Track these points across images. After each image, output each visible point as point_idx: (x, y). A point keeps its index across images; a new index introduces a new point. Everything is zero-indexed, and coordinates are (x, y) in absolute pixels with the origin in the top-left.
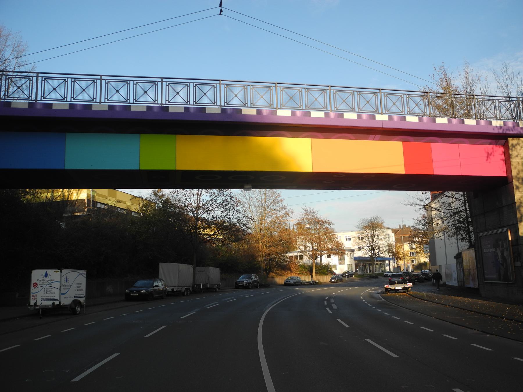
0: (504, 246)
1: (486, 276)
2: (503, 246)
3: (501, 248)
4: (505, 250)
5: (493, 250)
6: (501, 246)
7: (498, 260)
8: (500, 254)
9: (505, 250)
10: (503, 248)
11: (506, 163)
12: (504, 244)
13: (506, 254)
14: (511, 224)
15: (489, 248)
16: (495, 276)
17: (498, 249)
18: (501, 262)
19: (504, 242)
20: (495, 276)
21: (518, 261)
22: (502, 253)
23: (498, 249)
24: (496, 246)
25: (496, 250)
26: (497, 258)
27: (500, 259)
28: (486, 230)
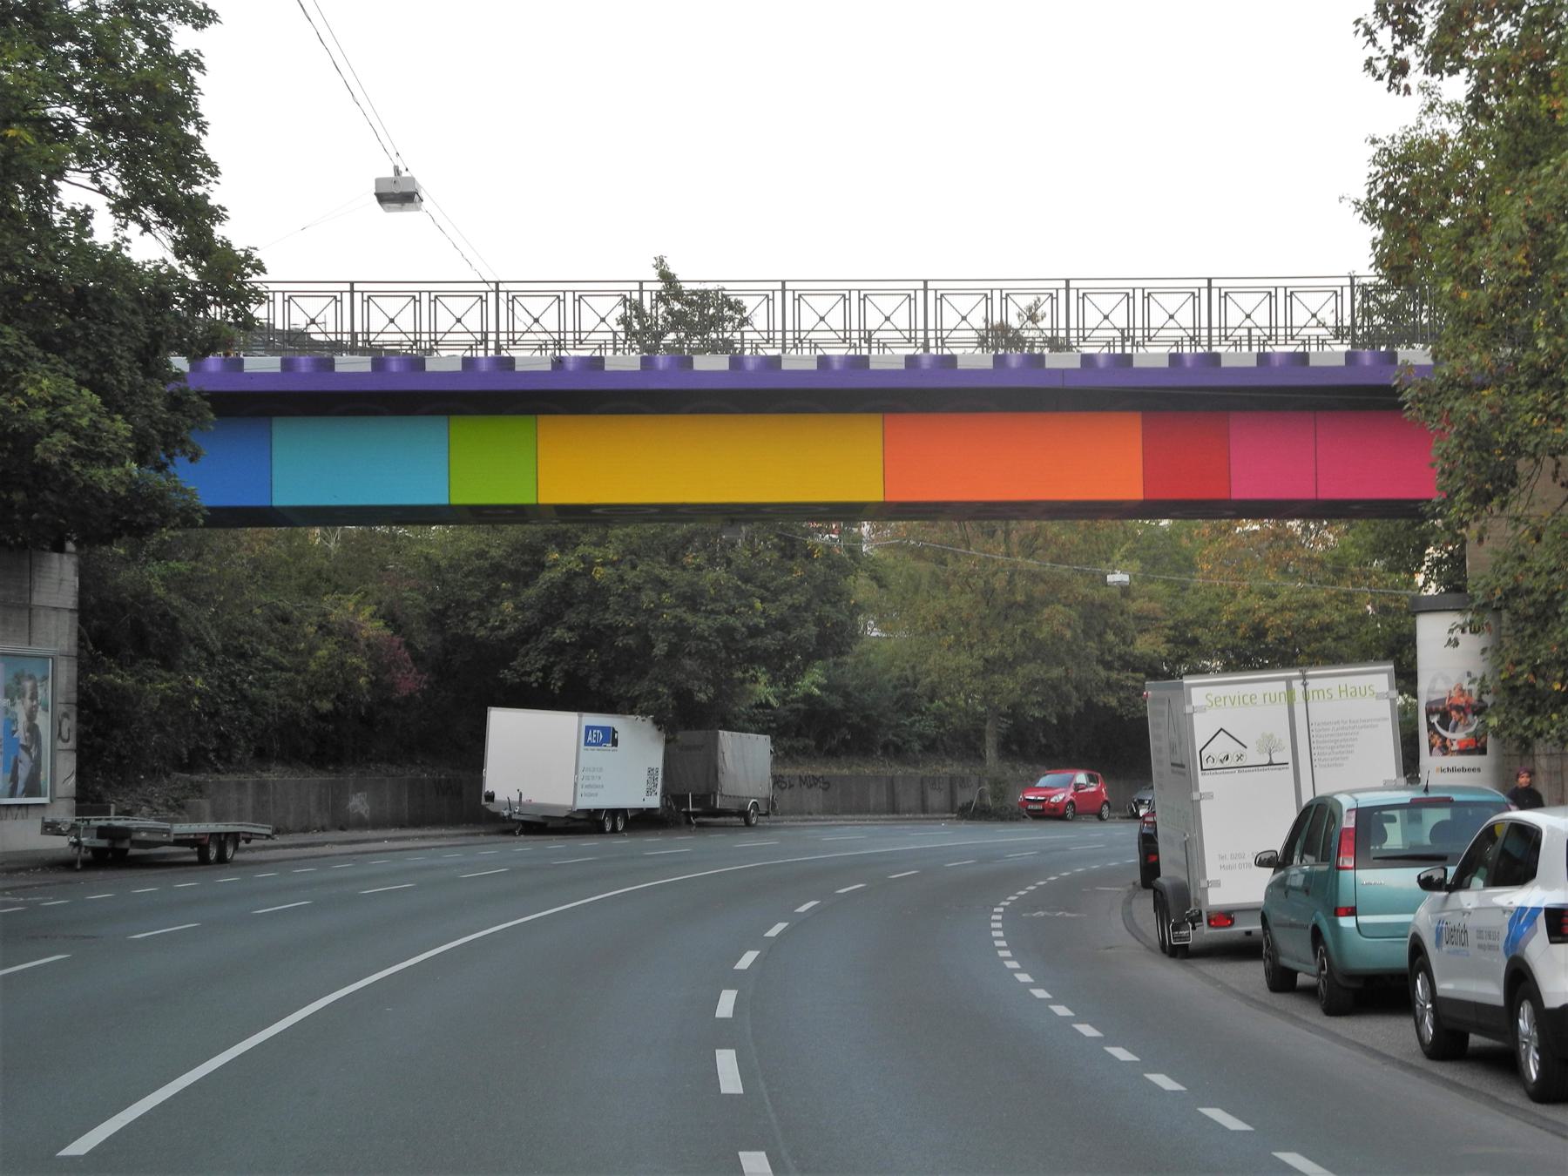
0: (39, 698)
2: (34, 697)
3: (28, 702)
6: (28, 694)
7: (15, 736)
8: (22, 719)
9: (40, 708)
10: (35, 703)
12: (40, 691)
17: (18, 701)
18: (22, 742)
22: (31, 716)
23: (18, 701)
25: (13, 704)
26: (14, 729)
27: (21, 734)
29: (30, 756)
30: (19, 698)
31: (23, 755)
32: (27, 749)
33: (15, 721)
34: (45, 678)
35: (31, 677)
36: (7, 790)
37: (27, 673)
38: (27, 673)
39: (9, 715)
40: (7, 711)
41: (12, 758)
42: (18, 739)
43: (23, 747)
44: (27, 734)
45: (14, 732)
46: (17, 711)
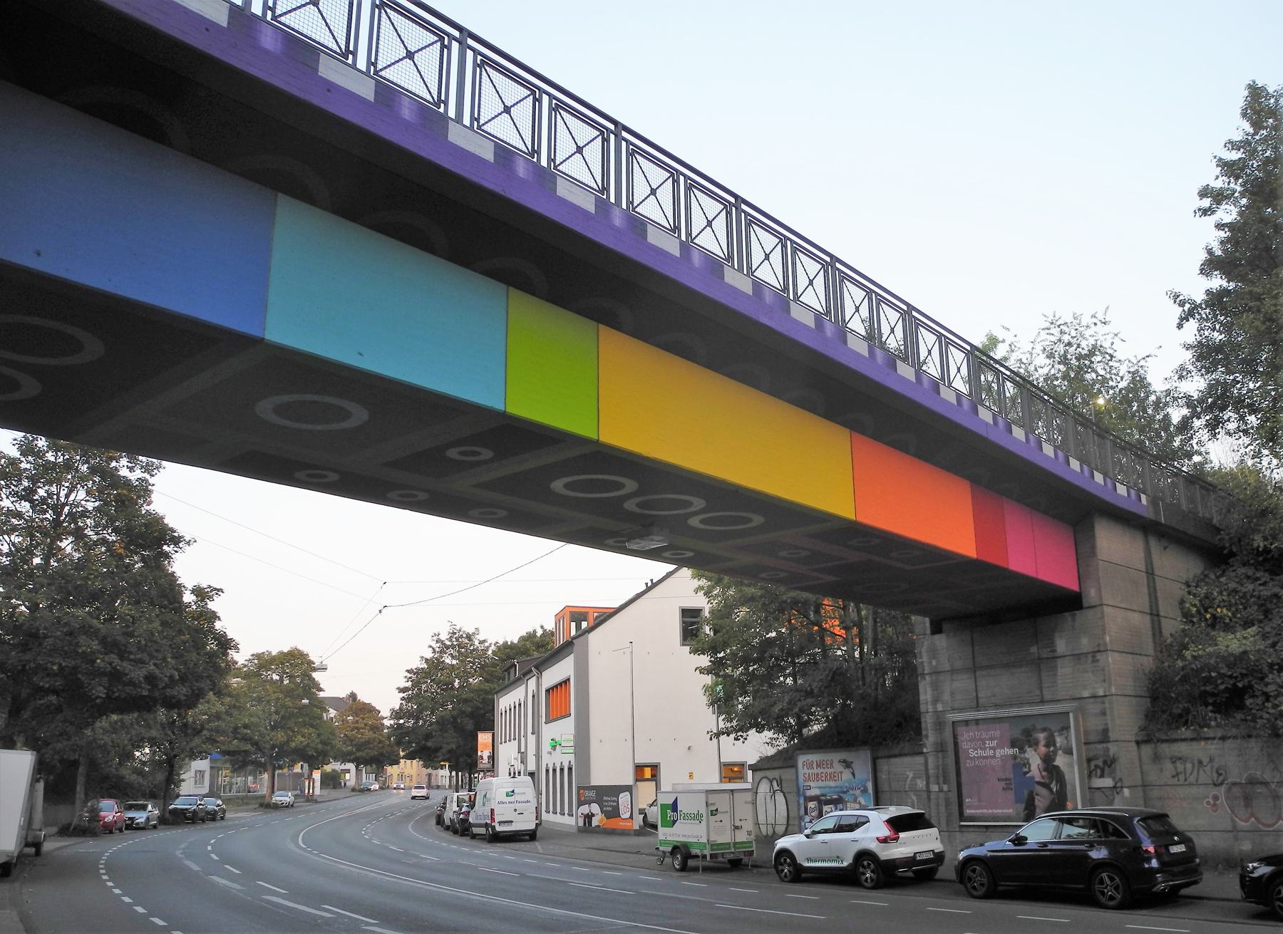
1: (968, 812)
2: (1050, 742)
3: (1042, 749)
4: (1060, 752)
5: (1010, 751)
6: (1043, 742)
9: (1060, 752)
10: (1052, 749)
11: (1080, 562)
13: (1060, 761)
14: (1086, 694)
15: (994, 749)
16: (1011, 811)
18: (1037, 780)
19: (1055, 734)
20: (1011, 811)
21: (1102, 776)
22: (1048, 760)
24: (1023, 740)
25: (1022, 750)
26: (1027, 770)
28: (978, 707)
29: (1051, 790)
30: (1030, 746)
31: (1039, 789)
32: (1045, 785)
33: (1027, 764)
34: (1067, 728)
35: (1044, 730)
36: (1022, 815)
37: (1039, 727)
38: (1039, 727)
39: (1018, 760)
40: (1015, 757)
41: (1026, 793)
42: (1033, 778)
43: (1039, 783)
44: (1044, 773)
45: (1028, 773)
46: (1027, 755)
